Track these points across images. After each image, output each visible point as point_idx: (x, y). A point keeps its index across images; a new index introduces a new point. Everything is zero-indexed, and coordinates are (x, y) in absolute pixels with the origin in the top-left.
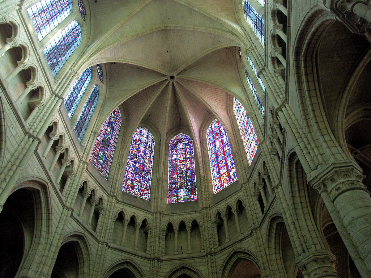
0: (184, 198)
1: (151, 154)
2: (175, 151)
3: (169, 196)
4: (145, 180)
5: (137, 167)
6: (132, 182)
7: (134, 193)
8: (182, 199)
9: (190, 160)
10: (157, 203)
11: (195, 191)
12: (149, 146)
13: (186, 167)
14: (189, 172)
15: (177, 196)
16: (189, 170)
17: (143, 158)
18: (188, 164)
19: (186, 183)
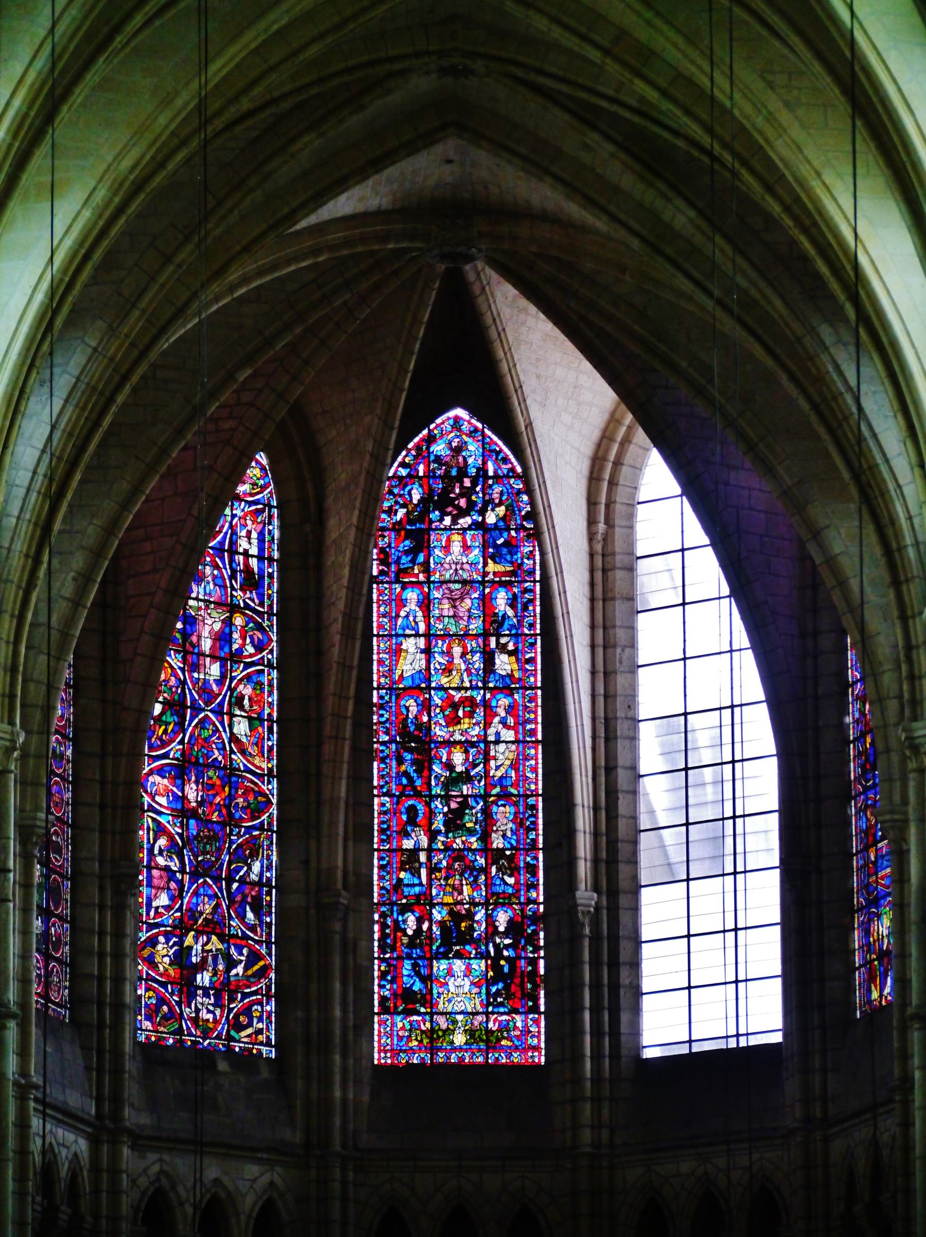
0: (471, 1033)
1: (259, 648)
2: (412, 595)
3: (383, 999)
4: (243, 902)
5: (193, 814)
6: (180, 943)
7: (195, 1021)
8: (459, 1039)
9: (511, 709)
10: (326, 1081)
11: (536, 987)
12: (248, 569)
13: (487, 772)
14: (504, 814)
15: (427, 999)
16: (505, 796)
17: (219, 712)
18: (497, 742)
19: (480, 915)
